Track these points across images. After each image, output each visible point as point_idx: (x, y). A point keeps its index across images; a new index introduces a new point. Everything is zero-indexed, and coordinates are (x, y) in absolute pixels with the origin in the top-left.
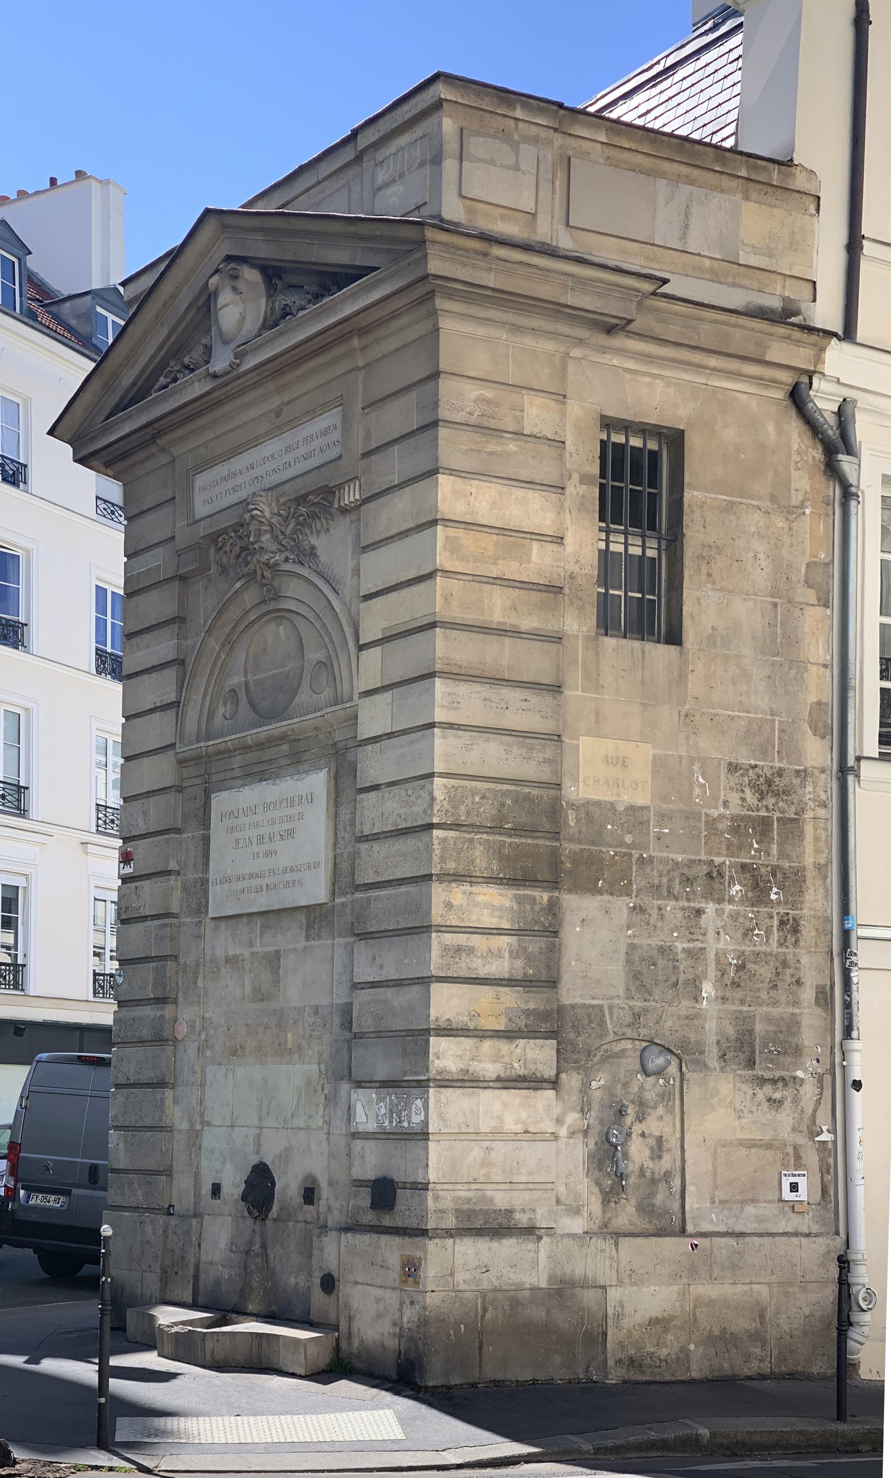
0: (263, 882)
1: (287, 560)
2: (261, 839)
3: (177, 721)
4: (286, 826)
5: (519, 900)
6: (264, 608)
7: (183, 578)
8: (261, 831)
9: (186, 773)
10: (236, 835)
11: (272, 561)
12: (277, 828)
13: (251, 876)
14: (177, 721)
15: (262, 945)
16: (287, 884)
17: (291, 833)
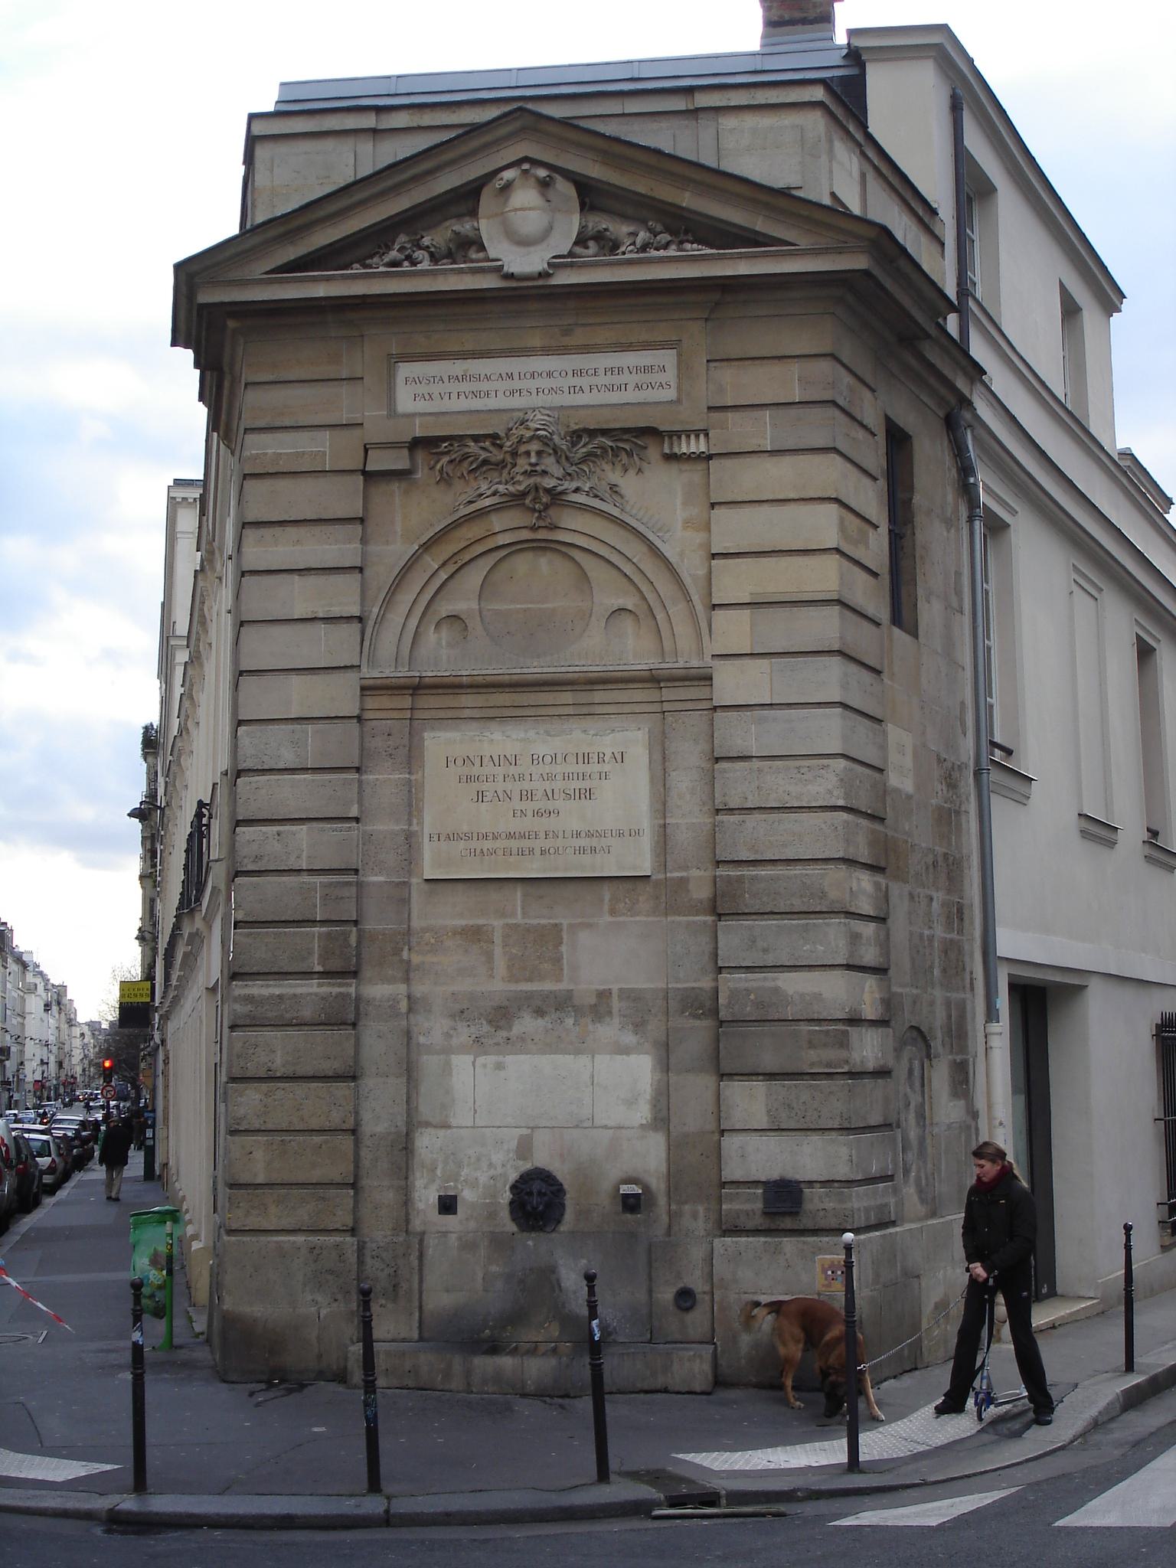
0: (538, 844)
1: (577, 490)
2: (530, 795)
3: (362, 641)
4: (586, 784)
5: (877, 885)
6: (525, 535)
7: (369, 476)
8: (526, 785)
9: (370, 703)
10: (475, 786)
11: (560, 489)
12: (559, 785)
13: (510, 836)
14: (362, 641)
15: (525, 914)
16: (582, 850)
17: (589, 794)
